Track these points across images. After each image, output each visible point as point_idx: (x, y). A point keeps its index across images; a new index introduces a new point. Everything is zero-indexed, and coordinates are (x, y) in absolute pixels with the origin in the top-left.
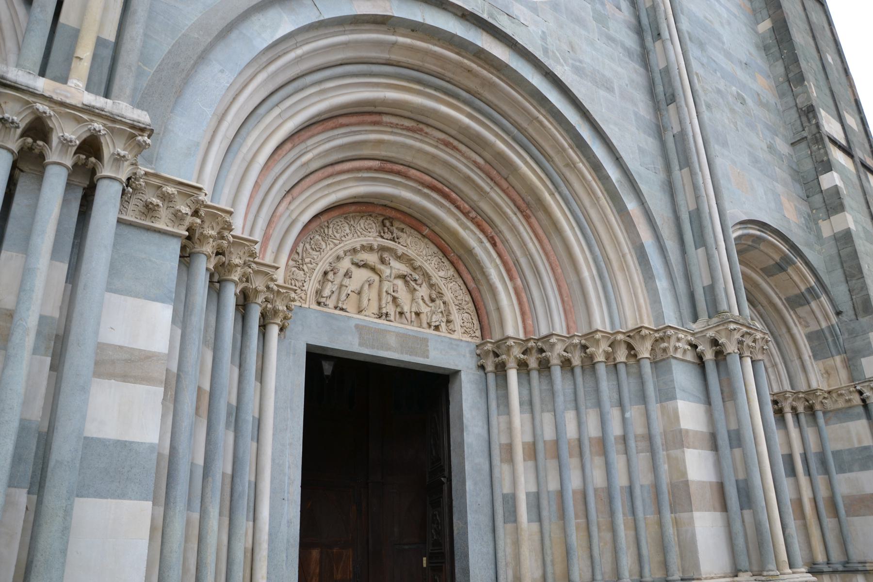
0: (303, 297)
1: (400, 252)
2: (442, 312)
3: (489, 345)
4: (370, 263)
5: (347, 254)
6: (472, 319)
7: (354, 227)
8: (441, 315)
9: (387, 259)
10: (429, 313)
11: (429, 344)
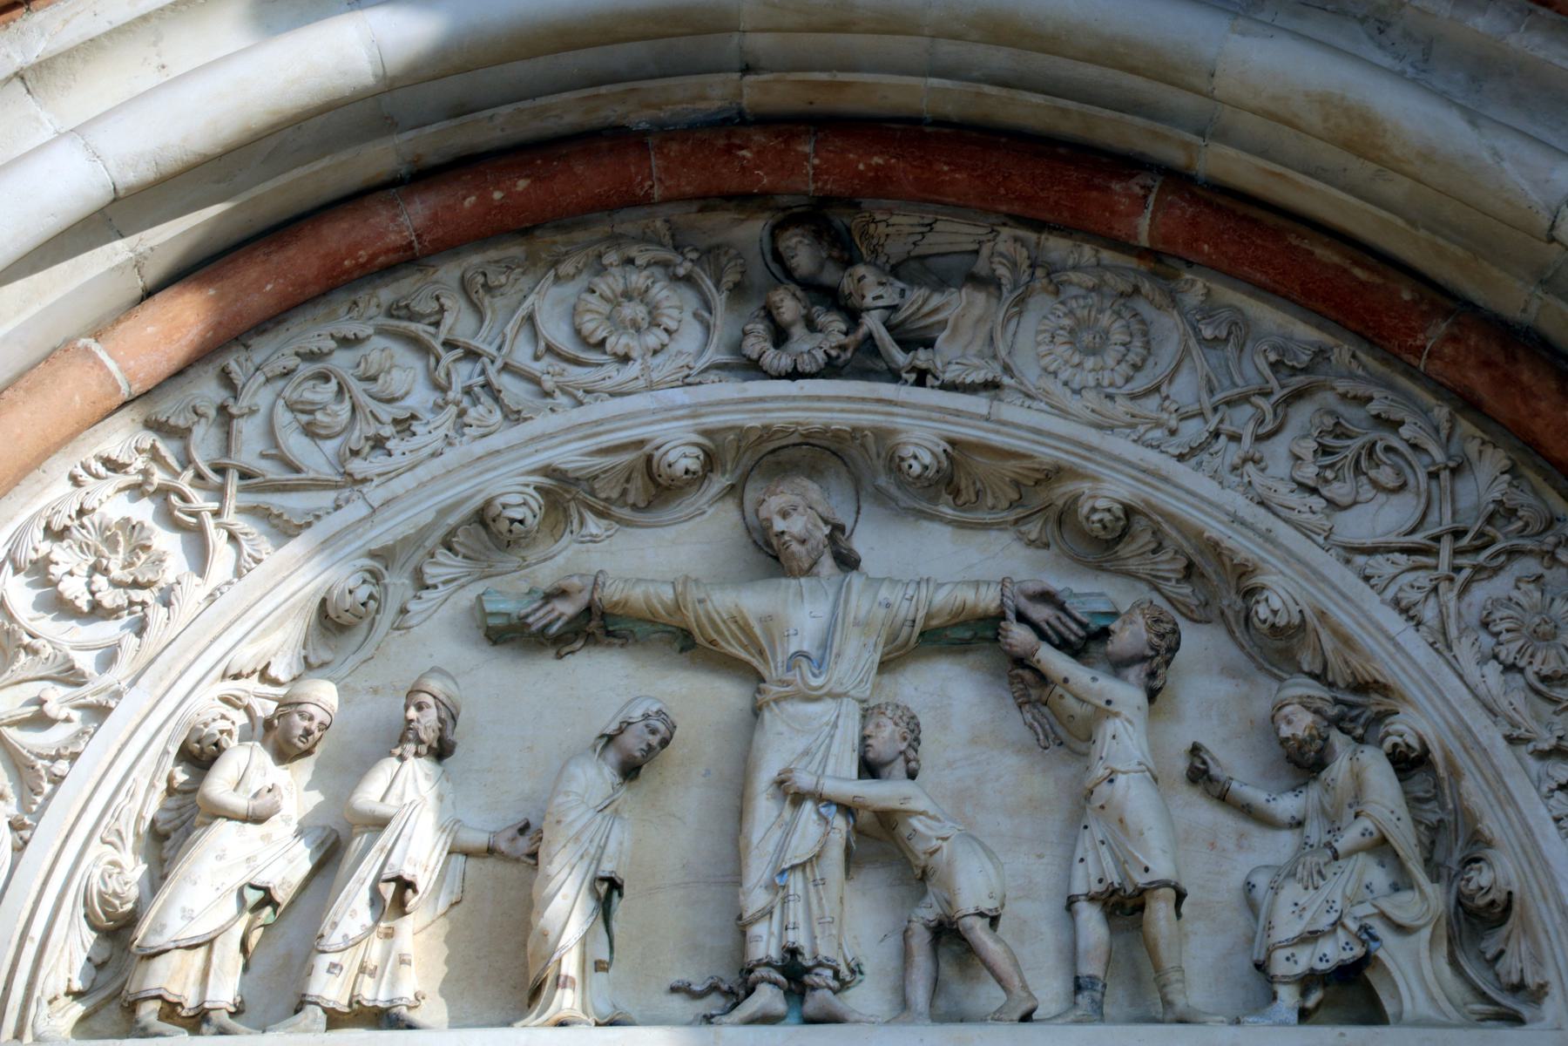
4: (637, 595)
5: (432, 572)
7: (472, 355)
8: (1379, 877)
9: (796, 525)
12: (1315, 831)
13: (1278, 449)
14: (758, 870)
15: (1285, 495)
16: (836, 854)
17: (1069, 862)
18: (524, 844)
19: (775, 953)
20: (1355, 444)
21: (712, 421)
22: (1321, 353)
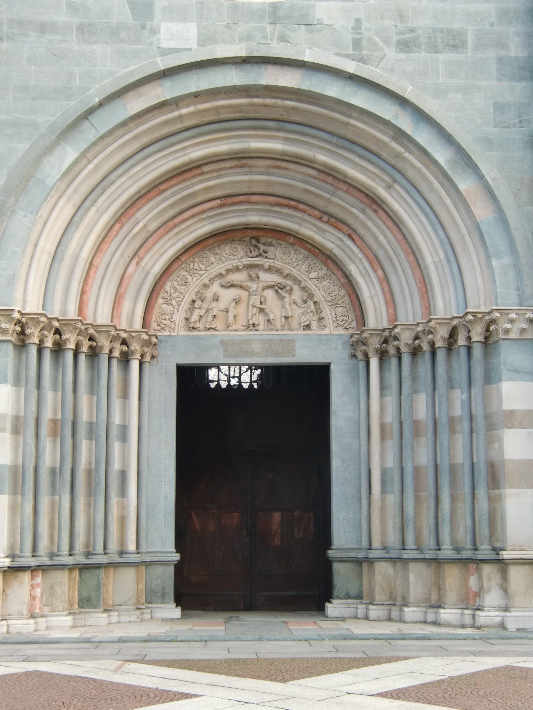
0: (172, 326)
1: (266, 266)
2: (312, 312)
3: (355, 336)
5: (215, 279)
6: (347, 312)
8: (311, 315)
9: (253, 275)
10: (300, 315)
11: (296, 344)
12: (306, 309)
13: (304, 267)
14: (250, 314)
15: (304, 272)
16: (258, 312)
17: (282, 312)
18: (226, 310)
19: (252, 323)
20: (312, 266)
21: (244, 263)
22: (308, 255)
